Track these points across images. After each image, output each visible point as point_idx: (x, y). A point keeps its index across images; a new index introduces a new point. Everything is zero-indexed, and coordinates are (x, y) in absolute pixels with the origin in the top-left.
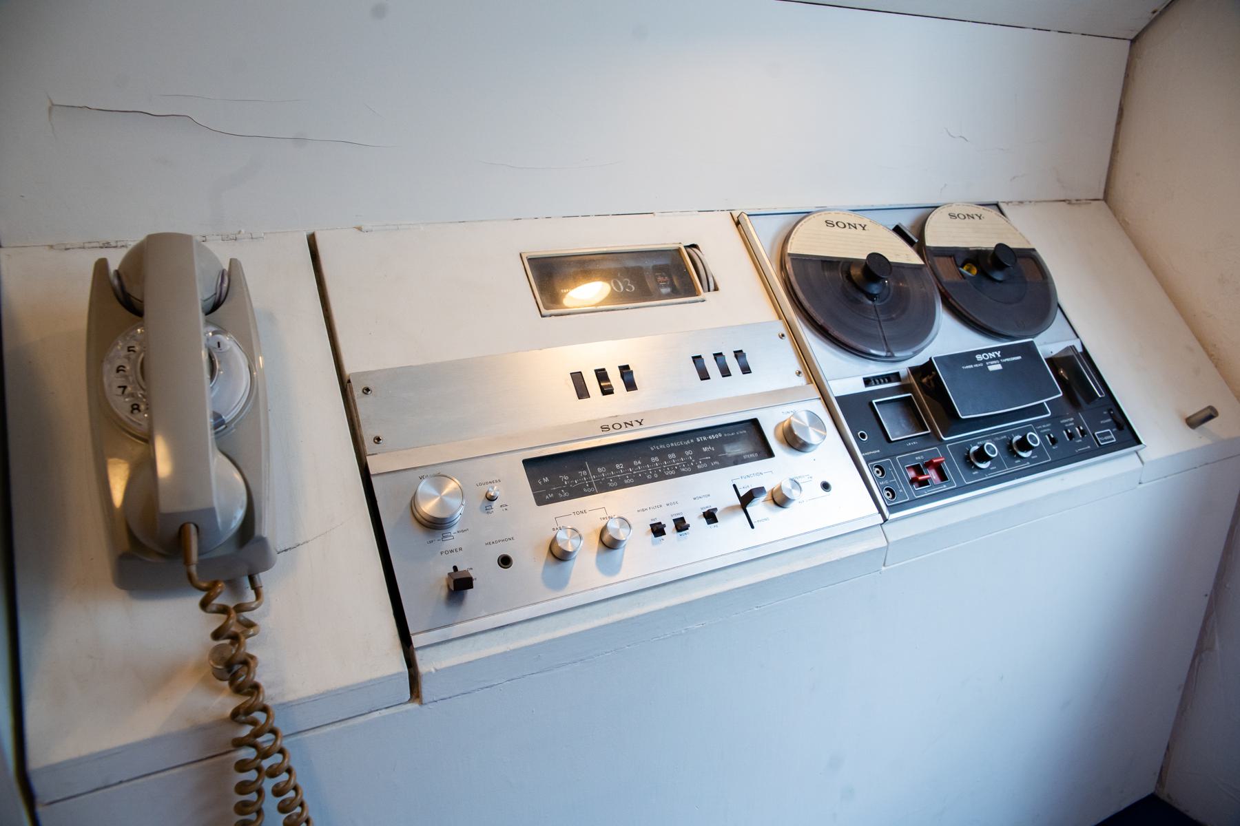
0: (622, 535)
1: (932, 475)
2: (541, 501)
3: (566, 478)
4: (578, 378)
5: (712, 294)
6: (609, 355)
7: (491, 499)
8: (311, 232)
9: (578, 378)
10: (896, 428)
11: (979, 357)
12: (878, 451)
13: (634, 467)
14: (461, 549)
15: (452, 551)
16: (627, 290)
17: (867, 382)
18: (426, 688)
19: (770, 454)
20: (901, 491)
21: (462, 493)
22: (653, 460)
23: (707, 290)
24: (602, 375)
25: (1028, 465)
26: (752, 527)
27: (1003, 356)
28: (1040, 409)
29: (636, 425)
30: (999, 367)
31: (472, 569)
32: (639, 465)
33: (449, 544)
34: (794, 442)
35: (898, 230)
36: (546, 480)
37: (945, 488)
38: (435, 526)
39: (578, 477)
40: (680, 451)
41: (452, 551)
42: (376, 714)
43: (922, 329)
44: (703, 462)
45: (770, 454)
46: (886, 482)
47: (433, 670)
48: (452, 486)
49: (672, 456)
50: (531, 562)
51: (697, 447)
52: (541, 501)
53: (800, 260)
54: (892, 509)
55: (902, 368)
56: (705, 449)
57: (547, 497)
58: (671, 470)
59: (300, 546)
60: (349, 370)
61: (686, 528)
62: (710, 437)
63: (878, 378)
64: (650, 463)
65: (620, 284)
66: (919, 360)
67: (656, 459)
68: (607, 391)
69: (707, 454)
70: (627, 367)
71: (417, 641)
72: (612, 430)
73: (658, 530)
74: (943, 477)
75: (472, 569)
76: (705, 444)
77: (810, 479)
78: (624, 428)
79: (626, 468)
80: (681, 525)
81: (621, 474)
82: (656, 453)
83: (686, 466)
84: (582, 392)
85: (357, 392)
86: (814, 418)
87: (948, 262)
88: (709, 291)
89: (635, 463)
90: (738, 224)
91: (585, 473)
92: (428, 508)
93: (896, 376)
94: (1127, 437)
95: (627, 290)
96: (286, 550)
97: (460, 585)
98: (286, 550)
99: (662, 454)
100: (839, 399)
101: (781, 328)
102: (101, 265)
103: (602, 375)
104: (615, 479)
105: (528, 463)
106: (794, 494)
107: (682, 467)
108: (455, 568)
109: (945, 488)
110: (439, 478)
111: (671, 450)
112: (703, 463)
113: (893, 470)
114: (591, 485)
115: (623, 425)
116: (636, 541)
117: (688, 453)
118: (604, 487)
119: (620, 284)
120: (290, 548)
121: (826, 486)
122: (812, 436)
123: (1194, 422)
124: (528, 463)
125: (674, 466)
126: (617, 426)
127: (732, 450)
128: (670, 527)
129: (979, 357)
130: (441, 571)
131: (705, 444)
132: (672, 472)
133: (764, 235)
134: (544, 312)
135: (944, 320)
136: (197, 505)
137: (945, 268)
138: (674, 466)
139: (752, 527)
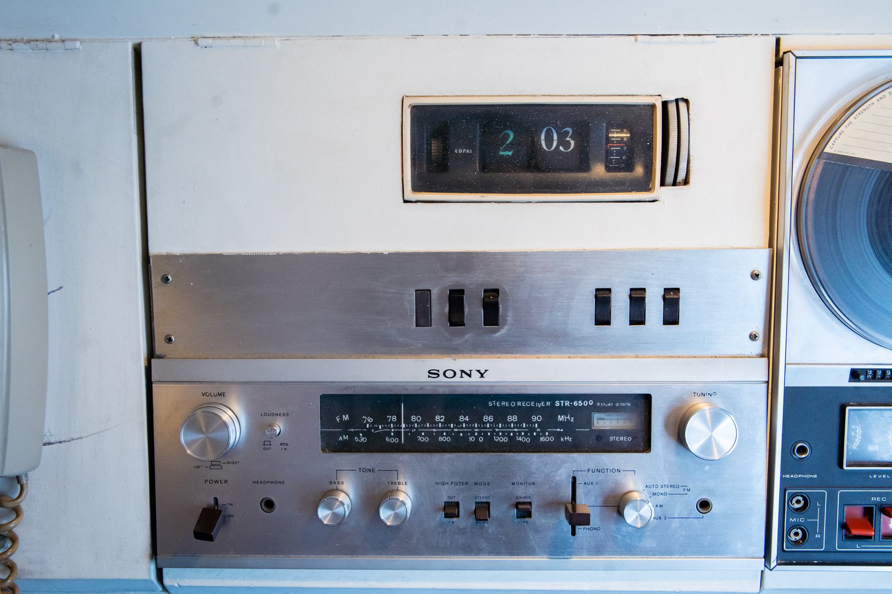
3: (370, 420)
8: (138, 41)
12: (815, 476)
14: (226, 481)
15: (216, 482)
16: (561, 148)
17: (855, 375)
22: (486, 418)
29: (476, 376)
31: (231, 505)
32: (465, 422)
36: (346, 418)
39: (385, 422)
41: (216, 482)
46: (802, 520)
47: (176, 585)
56: (561, 418)
57: (341, 438)
58: (503, 436)
59: (74, 441)
60: (153, 250)
64: (481, 422)
65: (555, 137)
67: (490, 418)
69: (561, 425)
75: (231, 505)
76: (563, 410)
77: (686, 492)
78: (457, 378)
79: (447, 421)
80: (482, 511)
81: (438, 428)
82: (494, 411)
83: (526, 435)
88: (675, 184)
89: (462, 418)
90: (779, 63)
91: (394, 418)
95: (561, 148)
96: (60, 442)
98: (60, 442)
101: (761, 261)
104: (428, 434)
107: (520, 435)
108: (216, 500)
112: (549, 436)
113: (822, 508)
114: (398, 434)
115: (459, 374)
117: (535, 418)
119: (555, 137)
120: (64, 441)
125: (509, 432)
131: (563, 410)
132: (505, 440)
134: (410, 195)
138: (509, 432)
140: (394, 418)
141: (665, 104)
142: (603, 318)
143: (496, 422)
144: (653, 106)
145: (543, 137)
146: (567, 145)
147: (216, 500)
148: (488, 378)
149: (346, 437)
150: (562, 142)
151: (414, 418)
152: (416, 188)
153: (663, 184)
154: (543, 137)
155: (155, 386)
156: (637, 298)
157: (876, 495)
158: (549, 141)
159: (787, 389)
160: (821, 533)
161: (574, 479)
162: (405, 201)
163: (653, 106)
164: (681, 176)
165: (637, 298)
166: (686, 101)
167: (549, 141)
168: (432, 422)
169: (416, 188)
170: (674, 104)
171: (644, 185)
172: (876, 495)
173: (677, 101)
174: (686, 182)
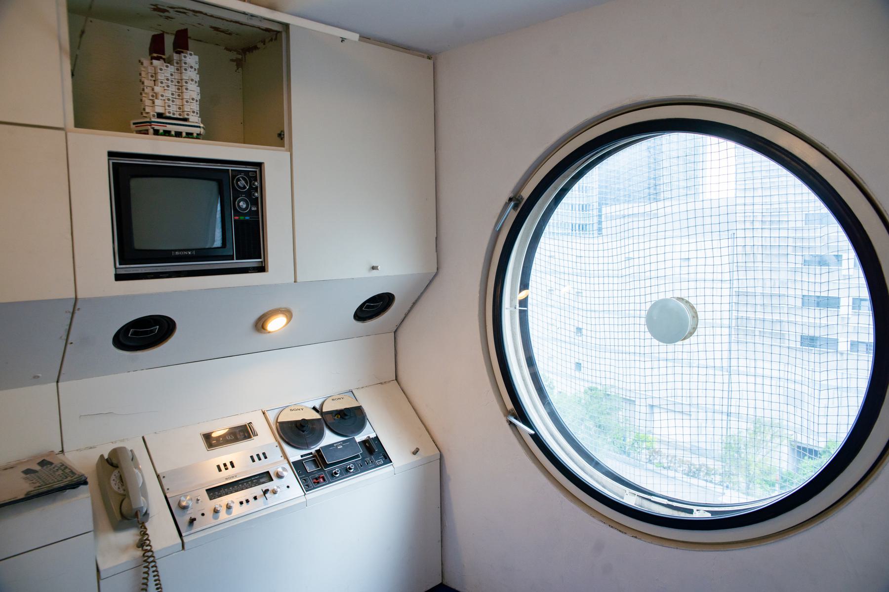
0: (232, 505)
1: (321, 480)
2: (211, 499)
4: (218, 467)
6: (227, 459)
7: (198, 500)
9: (218, 467)
10: (310, 468)
11: (335, 445)
17: (302, 456)
18: (186, 546)
19: (272, 480)
21: (191, 499)
24: (225, 465)
25: (352, 474)
27: (343, 443)
28: (357, 456)
30: (342, 447)
33: (188, 512)
34: (279, 476)
35: (314, 408)
37: (324, 483)
38: (184, 508)
40: (247, 482)
42: (174, 554)
43: (320, 436)
45: (272, 480)
48: (188, 498)
49: (245, 484)
50: (209, 514)
51: (252, 481)
52: (211, 499)
53: (282, 424)
54: (307, 491)
55: (313, 451)
61: (249, 502)
63: (306, 454)
66: (317, 448)
68: (227, 469)
70: (232, 462)
71: (183, 534)
73: (241, 503)
74: (324, 480)
80: (247, 501)
84: (220, 470)
85: (162, 478)
86: (284, 469)
87: (330, 415)
90: (264, 413)
92: (184, 504)
93: (311, 453)
94: (387, 460)
97: (192, 521)
99: (242, 484)
100: (292, 462)
101: (276, 444)
102: (102, 456)
103: (225, 465)
105: (207, 490)
106: (278, 490)
110: (186, 496)
118: (227, 494)
122: (285, 474)
123: (415, 452)
124: (207, 490)
127: (262, 480)
128: (245, 502)
129: (335, 445)
130: (187, 518)
133: (272, 416)
134: (208, 449)
135: (327, 433)
136: (140, 506)
137: (329, 419)
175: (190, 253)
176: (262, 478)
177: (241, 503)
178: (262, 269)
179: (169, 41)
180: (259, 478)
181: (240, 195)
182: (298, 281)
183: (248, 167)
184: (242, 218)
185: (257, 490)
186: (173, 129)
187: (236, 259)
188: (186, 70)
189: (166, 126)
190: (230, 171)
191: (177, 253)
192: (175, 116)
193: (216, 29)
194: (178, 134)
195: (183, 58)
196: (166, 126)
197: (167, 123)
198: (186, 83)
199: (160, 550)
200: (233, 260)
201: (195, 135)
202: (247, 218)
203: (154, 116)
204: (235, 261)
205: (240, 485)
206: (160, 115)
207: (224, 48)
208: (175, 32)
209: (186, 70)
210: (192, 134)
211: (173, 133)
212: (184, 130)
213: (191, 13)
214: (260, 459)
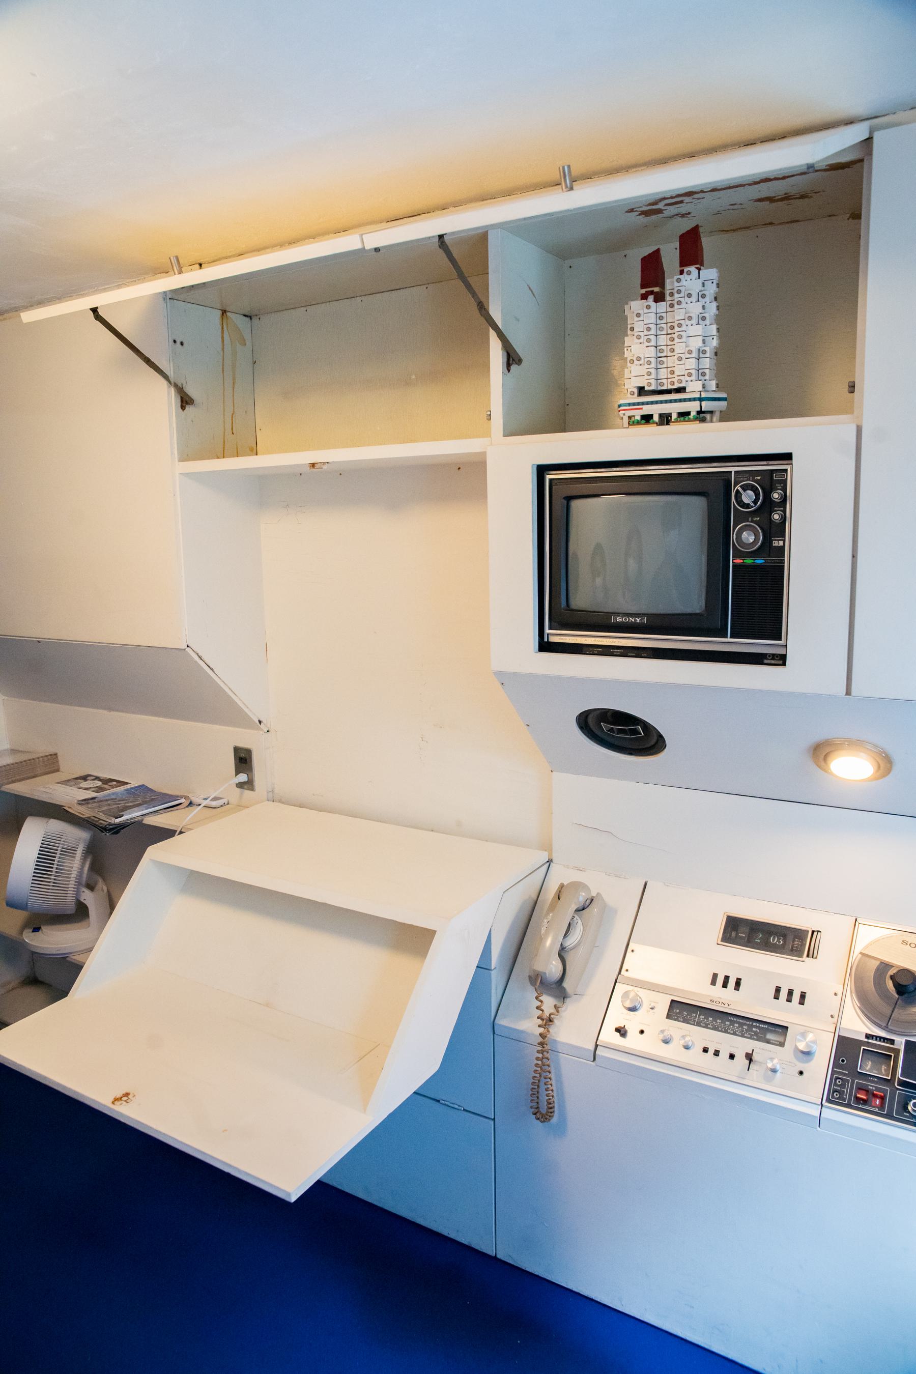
3: (686, 1014)
5: (810, 959)
8: (647, 880)
13: (716, 1022)
20: (845, 1097)
23: (811, 957)
26: (748, 1070)
29: (726, 1005)
36: (678, 1011)
40: (741, 1025)
42: (582, 1060)
44: (749, 1034)
46: (839, 1088)
49: (736, 1025)
54: (828, 1100)
56: (754, 1029)
61: (718, 1055)
62: (761, 1026)
63: (877, 1037)
64: (725, 1023)
65: (776, 939)
67: (729, 1023)
69: (754, 1032)
70: (728, 977)
72: (714, 1003)
73: (705, 1050)
76: (756, 1027)
78: (720, 1005)
80: (717, 1053)
82: (730, 1021)
84: (714, 982)
88: (813, 957)
91: (695, 1015)
108: (624, 1026)
109: (876, 1110)
111: (737, 1022)
114: (694, 1021)
115: (721, 1003)
116: (677, 1044)
117: (745, 1027)
119: (776, 939)
121: (642, 1032)
126: (718, 1002)
127: (770, 1036)
128: (711, 1051)
132: (732, 1032)
139: (748, 1070)
140: (695, 1015)
141: (813, 932)
142: (776, 997)
143: (730, 1025)
144: (808, 931)
145: (772, 938)
146: (780, 942)
147: (624, 1026)
148: (730, 1007)
149: (676, 1017)
150: (778, 941)
151: (701, 1017)
152: (722, 941)
153: (808, 956)
154: (772, 938)
155: (617, 984)
156: (790, 993)
157: (871, 1086)
158: (773, 940)
159: (839, 1036)
160: (846, 1096)
161: (753, 1050)
162: (718, 944)
163: (808, 931)
164: (815, 956)
165: (790, 993)
166: (820, 932)
167: (773, 940)
168: (708, 1020)
169: (722, 941)
170: (817, 933)
171: (800, 955)
172: (871, 1086)
173: (818, 931)
174: (816, 958)
175: (638, 621)
176: (771, 1031)
177: (705, 1050)
178: (781, 660)
179: (670, 256)
180: (767, 1030)
181: (750, 519)
182: (853, 693)
183: (771, 463)
184: (749, 561)
185: (742, 1045)
186: (655, 410)
187: (731, 638)
188: (679, 303)
189: (642, 409)
190: (733, 473)
191: (619, 619)
192: (665, 388)
193: (771, 199)
194: (665, 419)
195: (676, 284)
196: (642, 409)
197: (643, 404)
198: (680, 325)
199: (563, 1043)
200: (727, 637)
201: (693, 414)
202: (760, 561)
203: (632, 394)
204: (729, 639)
205: (728, 1023)
206: (641, 391)
207: (849, 215)
208: (702, 235)
209: (679, 303)
210: (688, 413)
211: (656, 418)
212: (674, 409)
213: (687, 199)
214: (789, 1000)
